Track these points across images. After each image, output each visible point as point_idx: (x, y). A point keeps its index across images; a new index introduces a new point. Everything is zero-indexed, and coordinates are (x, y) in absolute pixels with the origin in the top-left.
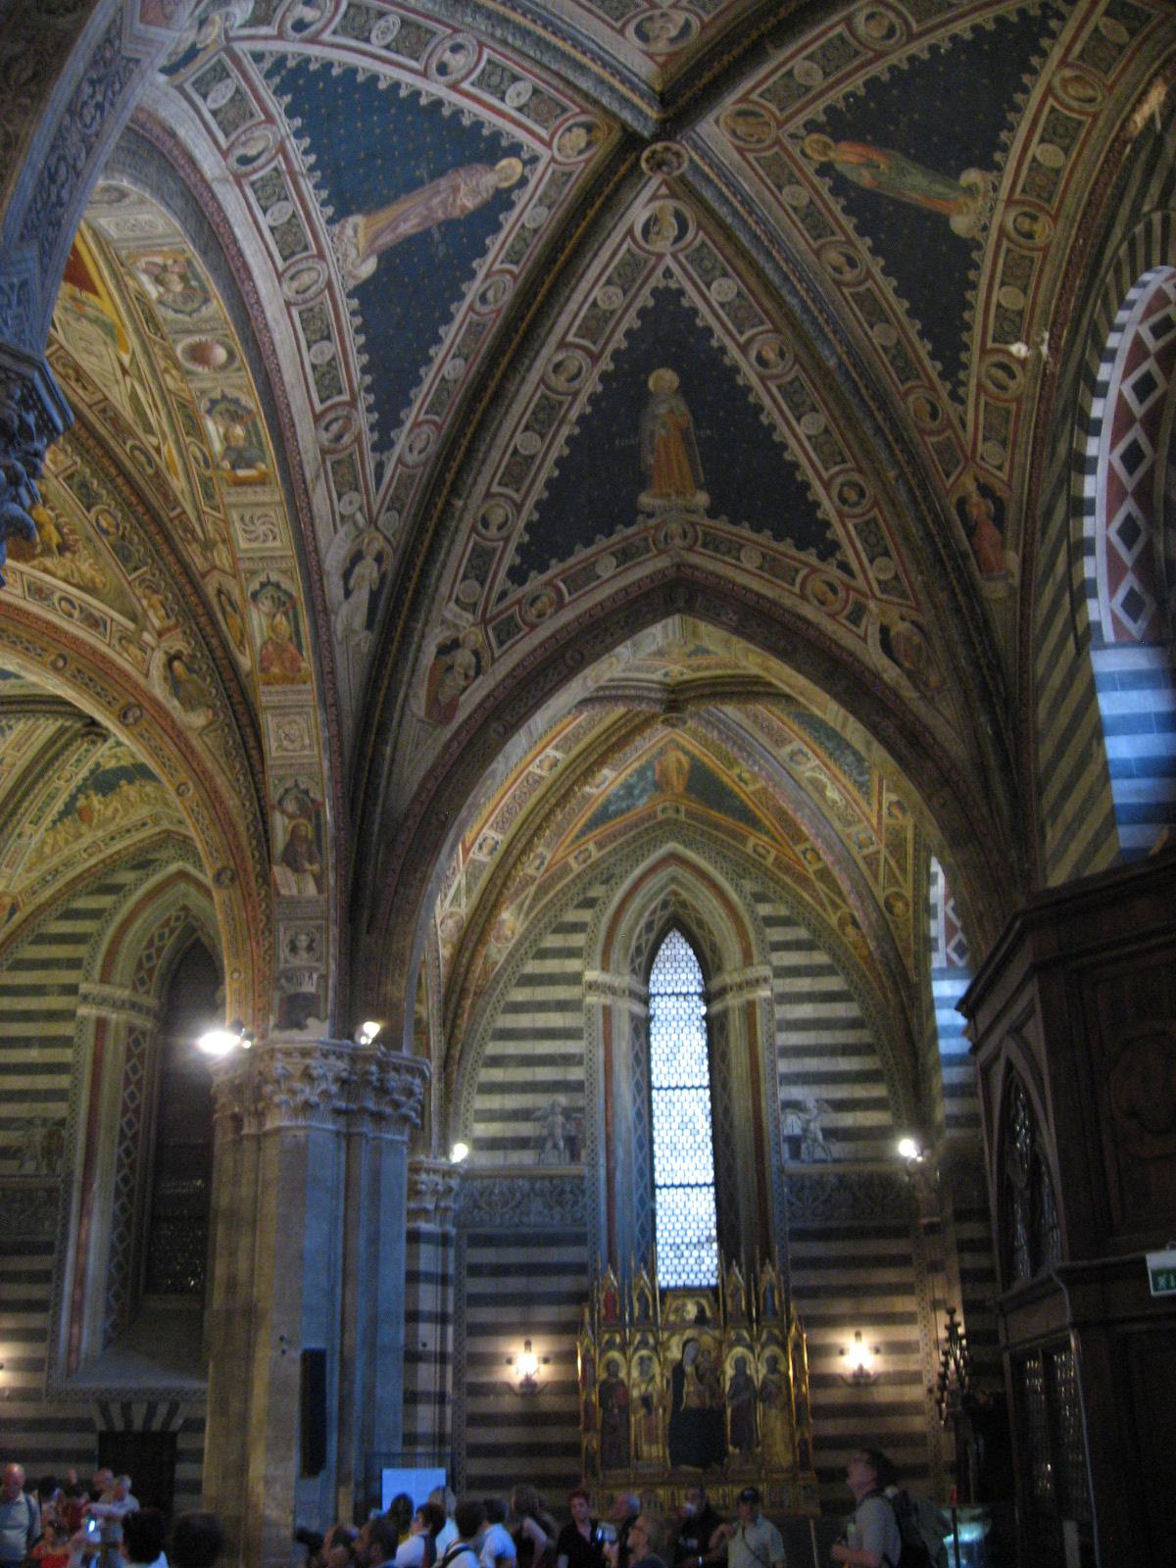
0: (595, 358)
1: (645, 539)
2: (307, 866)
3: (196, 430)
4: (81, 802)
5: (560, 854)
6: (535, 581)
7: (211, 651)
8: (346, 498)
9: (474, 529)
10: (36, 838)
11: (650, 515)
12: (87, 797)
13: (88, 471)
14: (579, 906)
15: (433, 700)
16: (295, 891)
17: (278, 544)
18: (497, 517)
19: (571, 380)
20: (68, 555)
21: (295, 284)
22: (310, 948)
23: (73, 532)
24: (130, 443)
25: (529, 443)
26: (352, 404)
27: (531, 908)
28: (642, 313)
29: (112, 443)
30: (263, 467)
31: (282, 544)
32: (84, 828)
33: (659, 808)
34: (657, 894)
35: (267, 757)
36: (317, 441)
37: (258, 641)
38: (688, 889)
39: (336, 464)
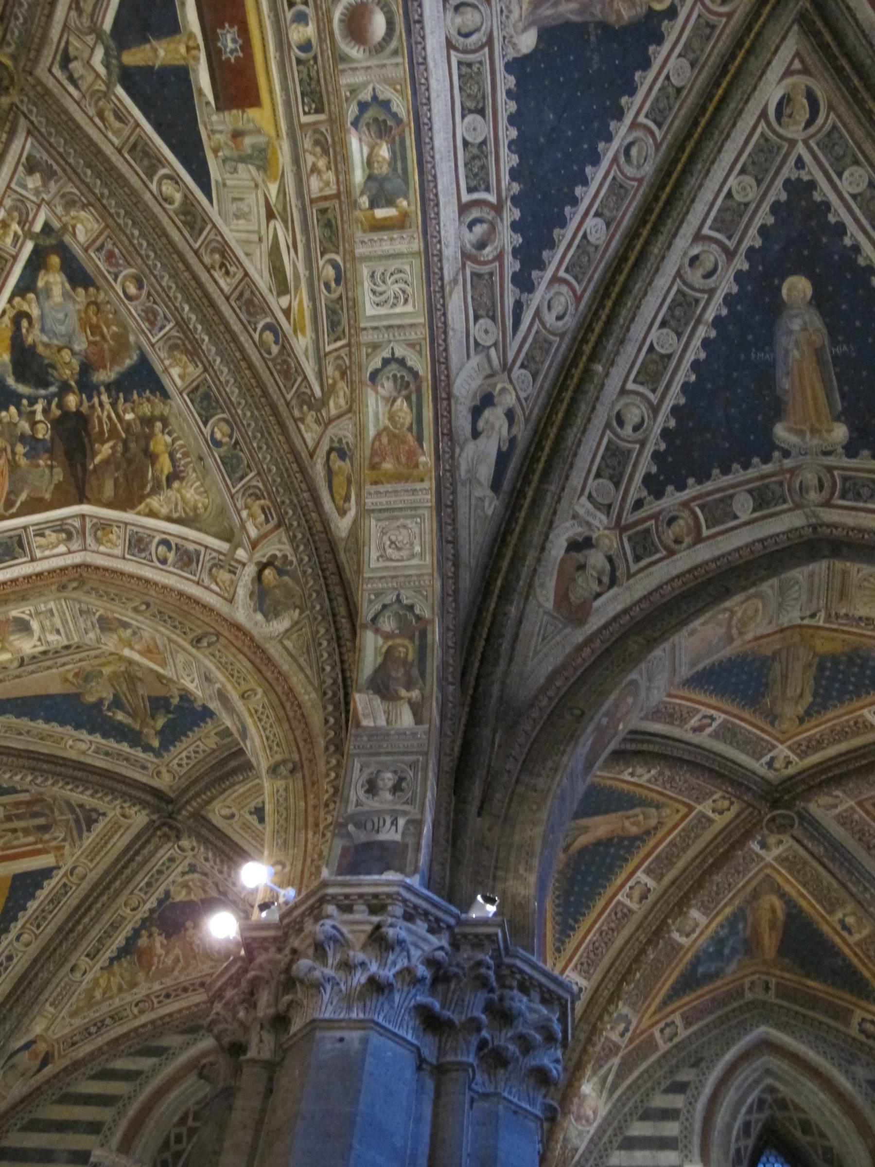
0: (730, 254)
1: (781, 484)
2: (403, 693)
3: (338, 157)
4: (143, 942)
5: (646, 1022)
6: (672, 499)
7: (310, 528)
8: (481, 321)
9: (608, 426)
10: (89, 977)
11: (786, 454)
12: (150, 936)
14: (667, 1091)
15: (562, 597)
16: (382, 722)
17: (409, 308)
18: (633, 416)
19: (708, 275)
20: (176, 484)
21: (458, 20)
22: (397, 788)
23: (186, 455)
24: (260, 326)
25: (665, 341)
26: (498, 208)
27: (615, 1086)
28: (776, 208)
29: (243, 338)
30: (405, 203)
31: (412, 310)
32: (141, 976)
33: (747, 982)
34: (751, 1088)
35: (366, 568)
36: (459, 237)
37: (372, 433)
38: (786, 1083)
39: (475, 275)
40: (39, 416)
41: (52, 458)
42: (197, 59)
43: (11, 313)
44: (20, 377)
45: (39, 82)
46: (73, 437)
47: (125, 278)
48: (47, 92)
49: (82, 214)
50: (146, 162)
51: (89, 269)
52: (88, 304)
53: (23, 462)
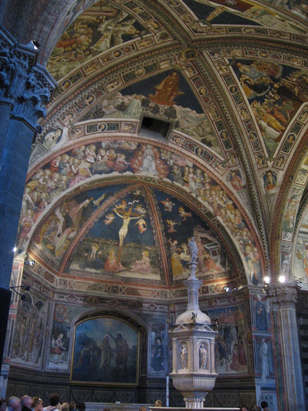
13: (289, 54)
40: (273, 96)
41: (285, 101)
42: (226, 9)
43: (243, 83)
44: (260, 93)
45: (196, 41)
46: (285, 93)
47: (260, 54)
48: (200, 40)
49: (234, 51)
50: (236, 30)
51: (249, 59)
52: (257, 65)
53: (280, 107)
